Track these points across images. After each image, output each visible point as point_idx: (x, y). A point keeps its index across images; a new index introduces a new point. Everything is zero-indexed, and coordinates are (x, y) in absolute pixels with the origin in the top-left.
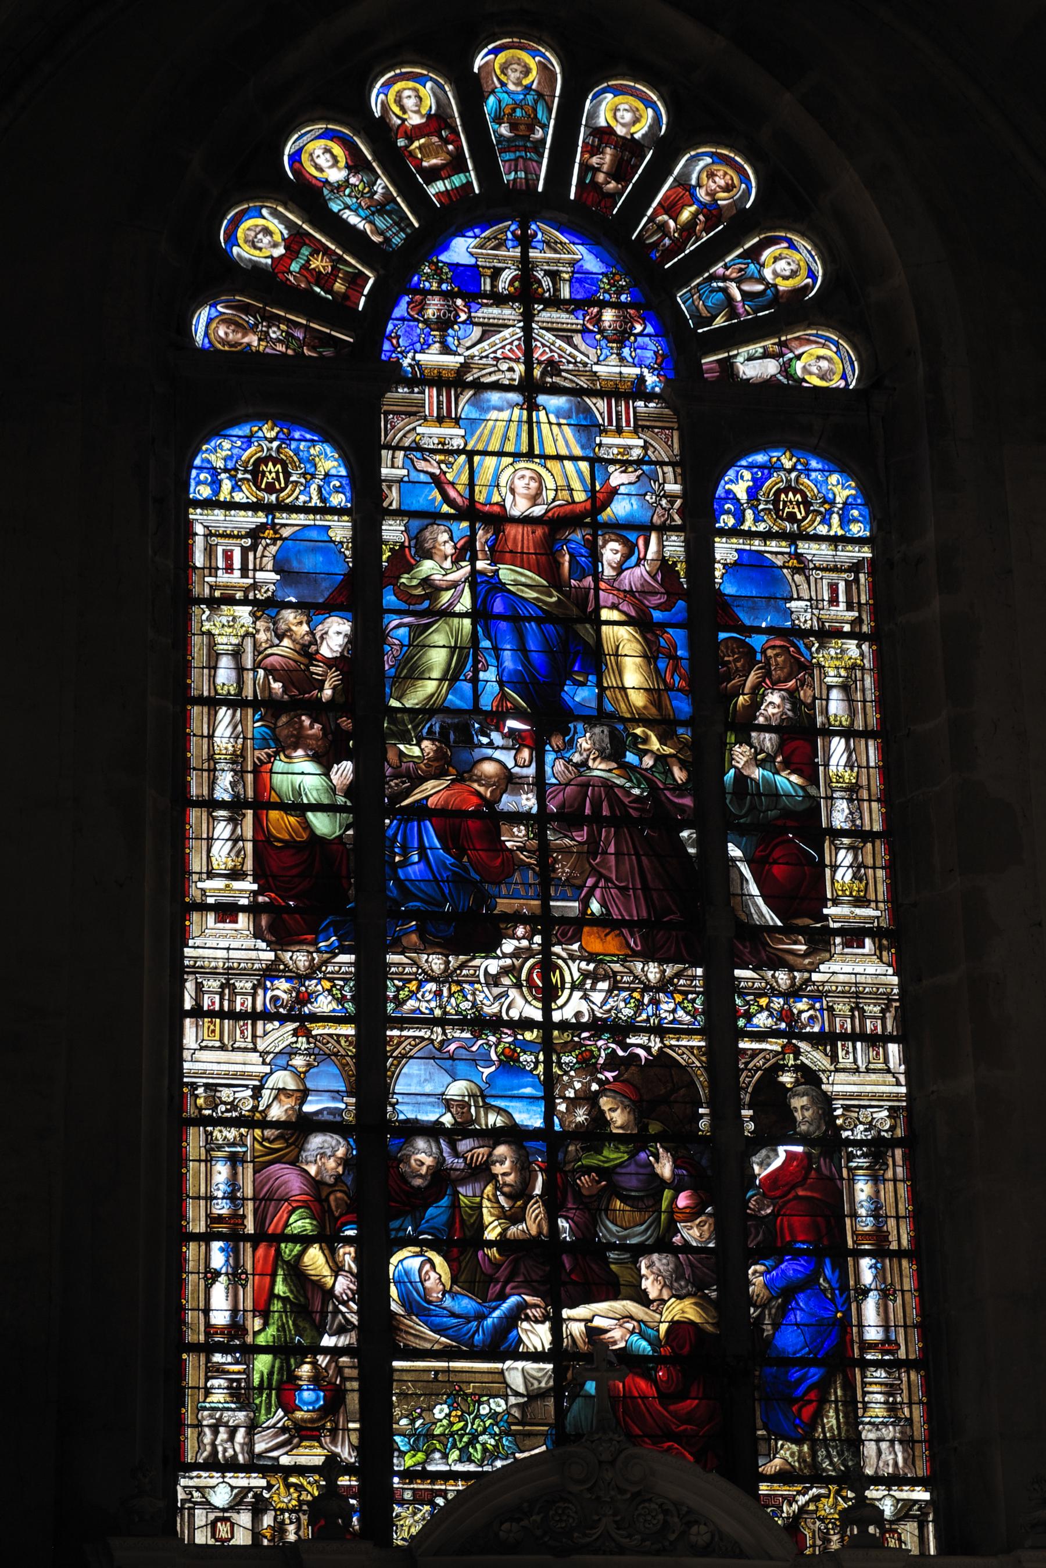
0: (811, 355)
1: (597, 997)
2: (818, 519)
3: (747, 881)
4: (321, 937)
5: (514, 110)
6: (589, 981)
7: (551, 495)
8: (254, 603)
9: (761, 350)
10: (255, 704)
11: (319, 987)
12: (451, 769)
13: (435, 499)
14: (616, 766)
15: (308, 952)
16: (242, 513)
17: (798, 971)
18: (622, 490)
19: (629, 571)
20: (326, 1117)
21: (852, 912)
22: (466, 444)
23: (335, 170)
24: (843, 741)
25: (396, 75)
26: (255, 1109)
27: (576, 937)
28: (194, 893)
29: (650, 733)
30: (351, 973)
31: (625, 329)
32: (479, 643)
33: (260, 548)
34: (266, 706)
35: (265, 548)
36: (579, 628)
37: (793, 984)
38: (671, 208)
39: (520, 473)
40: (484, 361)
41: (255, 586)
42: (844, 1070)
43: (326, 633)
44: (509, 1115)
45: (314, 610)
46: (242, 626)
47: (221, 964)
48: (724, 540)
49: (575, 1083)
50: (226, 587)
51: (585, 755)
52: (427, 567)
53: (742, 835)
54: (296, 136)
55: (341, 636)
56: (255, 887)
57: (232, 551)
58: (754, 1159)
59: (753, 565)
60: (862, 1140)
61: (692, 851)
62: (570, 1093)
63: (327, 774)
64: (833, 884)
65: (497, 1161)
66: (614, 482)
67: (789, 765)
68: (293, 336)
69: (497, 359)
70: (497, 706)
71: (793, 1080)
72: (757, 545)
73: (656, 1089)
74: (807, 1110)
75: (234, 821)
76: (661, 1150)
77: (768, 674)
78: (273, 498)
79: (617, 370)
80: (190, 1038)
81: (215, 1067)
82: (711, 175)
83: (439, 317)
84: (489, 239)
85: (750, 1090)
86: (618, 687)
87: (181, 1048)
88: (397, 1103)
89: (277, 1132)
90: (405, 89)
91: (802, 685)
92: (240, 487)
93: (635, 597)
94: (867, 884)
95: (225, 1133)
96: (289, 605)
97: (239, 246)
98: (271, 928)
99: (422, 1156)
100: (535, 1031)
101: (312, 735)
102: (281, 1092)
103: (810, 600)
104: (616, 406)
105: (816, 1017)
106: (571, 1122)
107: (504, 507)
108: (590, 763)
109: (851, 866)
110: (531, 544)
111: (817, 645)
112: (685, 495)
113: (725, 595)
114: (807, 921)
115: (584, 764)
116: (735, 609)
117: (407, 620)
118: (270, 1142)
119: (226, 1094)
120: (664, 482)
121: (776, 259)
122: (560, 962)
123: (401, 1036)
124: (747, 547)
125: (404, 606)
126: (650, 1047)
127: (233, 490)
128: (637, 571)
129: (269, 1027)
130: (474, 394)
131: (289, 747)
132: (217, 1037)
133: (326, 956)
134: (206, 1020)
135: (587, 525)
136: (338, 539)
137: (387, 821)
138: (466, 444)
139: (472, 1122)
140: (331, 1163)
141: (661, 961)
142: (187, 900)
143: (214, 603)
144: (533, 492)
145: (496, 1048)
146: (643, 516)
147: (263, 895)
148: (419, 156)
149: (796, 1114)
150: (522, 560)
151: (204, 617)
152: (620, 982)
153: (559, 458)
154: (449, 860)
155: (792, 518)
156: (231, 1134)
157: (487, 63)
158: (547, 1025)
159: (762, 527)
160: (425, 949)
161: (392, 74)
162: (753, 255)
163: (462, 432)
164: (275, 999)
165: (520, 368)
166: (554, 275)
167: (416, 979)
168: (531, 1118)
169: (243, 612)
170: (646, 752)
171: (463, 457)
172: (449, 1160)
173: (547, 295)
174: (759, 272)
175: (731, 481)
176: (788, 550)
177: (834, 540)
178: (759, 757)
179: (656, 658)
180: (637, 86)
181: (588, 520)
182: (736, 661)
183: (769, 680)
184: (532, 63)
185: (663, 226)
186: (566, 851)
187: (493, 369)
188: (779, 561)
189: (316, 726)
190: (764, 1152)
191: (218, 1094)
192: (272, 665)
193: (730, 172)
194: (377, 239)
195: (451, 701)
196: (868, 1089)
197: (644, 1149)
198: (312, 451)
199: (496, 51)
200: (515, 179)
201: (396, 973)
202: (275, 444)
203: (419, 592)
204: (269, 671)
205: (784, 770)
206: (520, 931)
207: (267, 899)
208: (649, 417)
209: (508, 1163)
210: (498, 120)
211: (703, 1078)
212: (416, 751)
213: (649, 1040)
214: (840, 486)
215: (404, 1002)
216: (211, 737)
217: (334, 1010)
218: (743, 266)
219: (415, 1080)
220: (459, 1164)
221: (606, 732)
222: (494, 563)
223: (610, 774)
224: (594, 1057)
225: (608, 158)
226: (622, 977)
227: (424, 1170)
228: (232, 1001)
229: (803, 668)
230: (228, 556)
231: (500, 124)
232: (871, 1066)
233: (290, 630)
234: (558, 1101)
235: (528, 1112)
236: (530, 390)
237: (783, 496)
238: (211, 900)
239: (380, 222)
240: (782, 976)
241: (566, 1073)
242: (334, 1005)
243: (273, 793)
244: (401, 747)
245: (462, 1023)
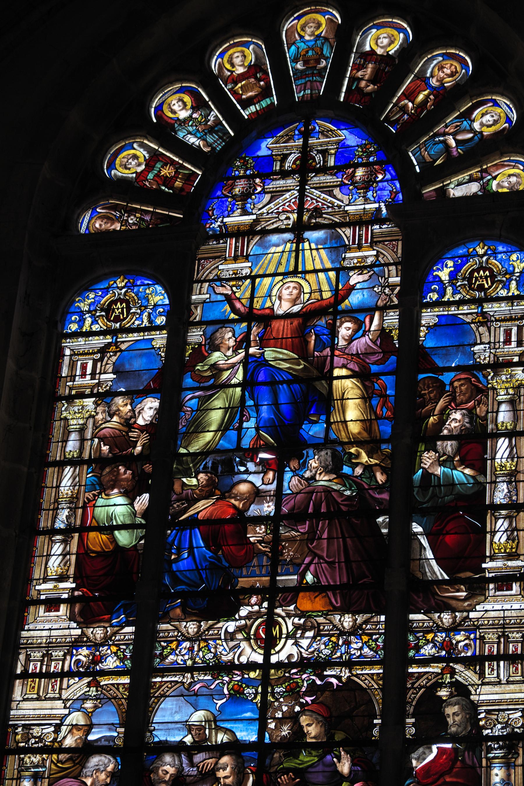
0: (504, 174)
1: (305, 643)
2: (501, 286)
3: (425, 548)
4: (114, 616)
5: (307, 52)
6: (299, 632)
7: (307, 296)
8: (98, 395)
9: (467, 178)
10: (89, 462)
11: (109, 651)
12: (217, 491)
13: (226, 310)
14: (335, 476)
15: (104, 627)
16: (97, 338)
17: (458, 612)
18: (358, 286)
19: (357, 341)
20: (104, 743)
21: (505, 565)
23: (184, 111)
24: (507, 440)
25: (230, 45)
26: (55, 740)
27: (294, 601)
28: (33, 593)
29: (361, 450)
30: (131, 639)
31: (371, 179)
32: (245, 403)
33: (106, 359)
34: (98, 462)
35: (109, 359)
36: (317, 384)
37: (454, 621)
38: (410, 95)
40: (270, 216)
41: (99, 384)
42: (488, 684)
43: (143, 409)
44: (233, 733)
45: (135, 395)
46: (88, 411)
47: (44, 641)
48: (429, 310)
49: (283, 707)
50: (80, 387)
51: (314, 472)
52: (216, 356)
53: (423, 516)
54: (161, 95)
55: (152, 410)
56: (74, 585)
57: (87, 363)
58: (413, 755)
59: (450, 325)
60: (499, 736)
61: (385, 531)
62: (279, 715)
63: (132, 504)
64: (491, 544)
65: (221, 768)
66: (352, 282)
67: (465, 462)
68: (143, 220)
69: (278, 213)
70: (253, 445)
71: (448, 693)
72: (453, 310)
73: (343, 708)
74: (458, 715)
75: (65, 542)
76: (343, 753)
77: (453, 399)
78: (118, 325)
79: (362, 207)
80: (17, 695)
81: (31, 712)
82: (441, 68)
83: (243, 192)
84: (282, 136)
85: (414, 703)
87: (11, 700)
88: (154, 730)
89: (67, 756)
90: (235, 53)
91: (479, 404)
92: (97, 321)
94: (518, 543)
95: (33, 759)
96: (121, 394)
97: (116, 169)
98: (82, 613)
99: (167, 768)
100: (258, 671)
101: (125, 478)
102: (75, 727)
103: (489, 343)
104: (359, 231)
105: (470, 645)
106: (277, 736)
107: (273, 309)
108: (317, 477)
109: (506, 531)
110: (289, 332)
111: (492, 374)
112: (402, 284)
113: (426, 348)
114: (469, 574)
115: (313, 478)
116: (433, 357)
117: (197, 394)
118: (63, 763)
119: (36, 731)
120: (389, 277)
121: (483, 115)
122: (280, 619)
123: (162, 682)
124: (446, 313)
125: (196, 385)
126: (342, 676)
127: (92, 324)
128: (363, 340)
129: (72, 681)
130: (260, 238)
131: (108, 488)
132: (36, 692)
133: (116, 629)
134: (30, 680)
135: (330, 313)
136: (158, 346)
137: (169, 532)
138: (251, 272)
139: (206, 740)
140: (103, 776)
141: (354, 613)
142: (28, 598)
143: (70, 399)
144: (294, 297)
145: (228, 685)
147: (78, 590)
148: (241, 92)
149: (448, 719)
150: (282, 343)
151: (63, 409)
152: (323, 630)
153: (315, 271)
154: (209, 554)
155: (481, 288)
156: (36, 759)
157: (292, 26)
158: (266, 666)
159: (457, 297)
160: (185, 618)
161: (228, 44)
162: (467, 115)
163: (249, 264)
164: (78, 661)
165: (294, 217)
166: (324, 153)
167: (177, 640)
168: (248, 734)
169: (89, 402)
170: (357, 464)
171: (249, 280)
172: (187, 769)
173: (318, 166)
174: (470, 126)
175: (438, 269)
176: (476, 311)
177: (511, 299)
178: (441, 459)
179: (370, 398)
180: (394, 20)
181: (331, 310)
182: (429, 393)
183: (455, 403)
184: (323, 20)
185: (404, 109)
186: (291, 540)
188: (468, 319)
189: (129, 472)
190: (421, 750)
191: (31, 731)
192: (104, 434)
193: (455, 64)
194: (206, 150)
195: (222, 445)
196: (508, 696)
197: (330, 752)
198: (147, 291)
199: (299, 18)
200: (303, 95)
201: (163, 637)
202: (124, 290)
203: (208, 374)
204: (101, 439)
205: (460, 466)
206: (254, 600)
207: (80, 593)
208: (382, 235)
209: (228, 769)
210: (295, 60)
211: (378, 696)
212: (194, 481)
213: (341, 671)
214: (519, 261)
215: (167, 657)
216: (58, 487)
217: (117, 667)
218: (459, 124)
219: (168, 713)
220: (194, 771)
221: (329, 454)
222: (262, 347)
223: (330, 483)
224: (299, 687)
225: (369, 70)
226: (324, 627)
227: (167, 777)
228: (48, 666)
229: (480, 392)
230: (84, 367)
231: (297, 63)
232: (511, 679)
233: (119, 410)
234: (269, 721)
235: (247, 730)
237: (476, 274)
238: (43, 597)
239: (210, 139)
240: (446, 616)
241: (277, 700)
242: (118, 663)
243: (94, 520)
244: (184, 480)
245: (206, 669)
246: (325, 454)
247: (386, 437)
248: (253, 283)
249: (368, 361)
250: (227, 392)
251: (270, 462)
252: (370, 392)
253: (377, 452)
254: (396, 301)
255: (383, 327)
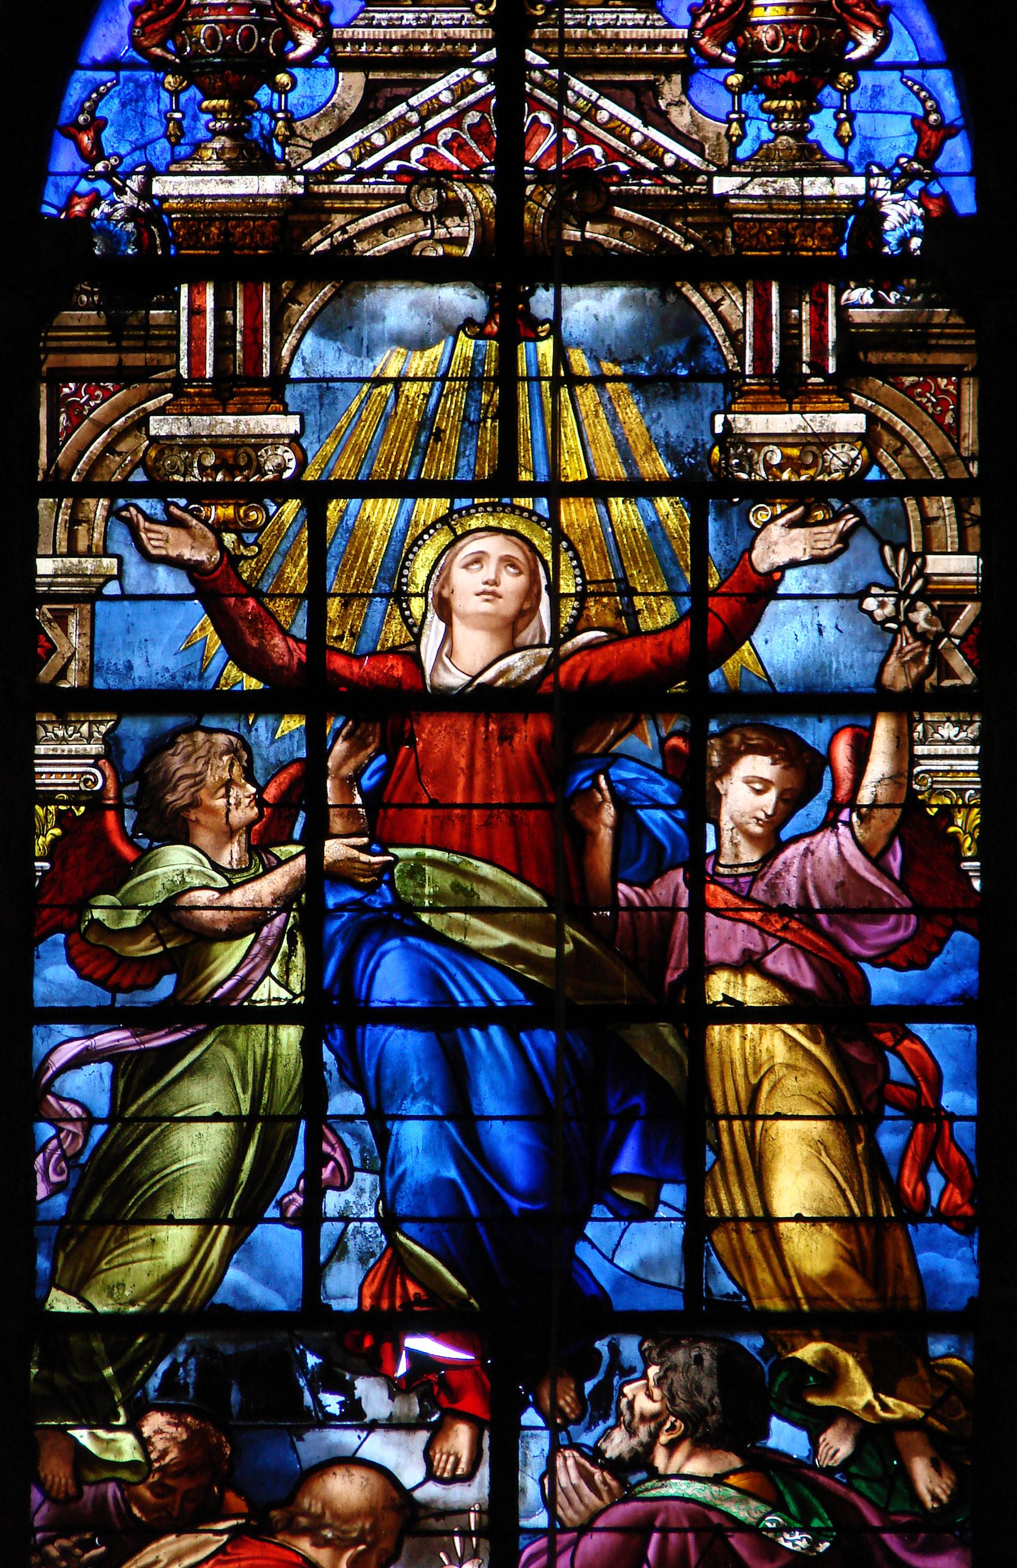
18: (792, 582)
22: (302, 464)
32: (324, 1100)
36: (638, 1035)
39: (471, 547)
51: (643, 1432)
66: (763, 559)
70: (377, 1297)
86: (751, 1218)
93: (816, 927)
107: (416, 659)
108: (660, 1459)
110: (499, 782)
112: (990, 588)
115: (641, 1460)
117: (106, 1040)
120: (927, 549)
125: (96, 996)
128: (826, 844)
130: (337, 295)
138: (302, 464)
144: (508, 606)
146: (852, 665)
163: (290, 424)
171: (292, 506)
179: (873, 1120)
187: (393, 211)
195: (237, 1291)
203: (145, 947)
208: (887, 336)
212: (126, 1447)
221: (707, 1360)
222: (380, 839)
236: (511, 268)
244: (82, 1436)
246: (694, 1359)
247: (954, 1301)
248: (315, 519)
249: (854, 946)
250: (240, 1041)
251: (455, 1379)
252: (869, 1090)
253: (914, 1370)
254: (963, 672)
255: (912, 794)
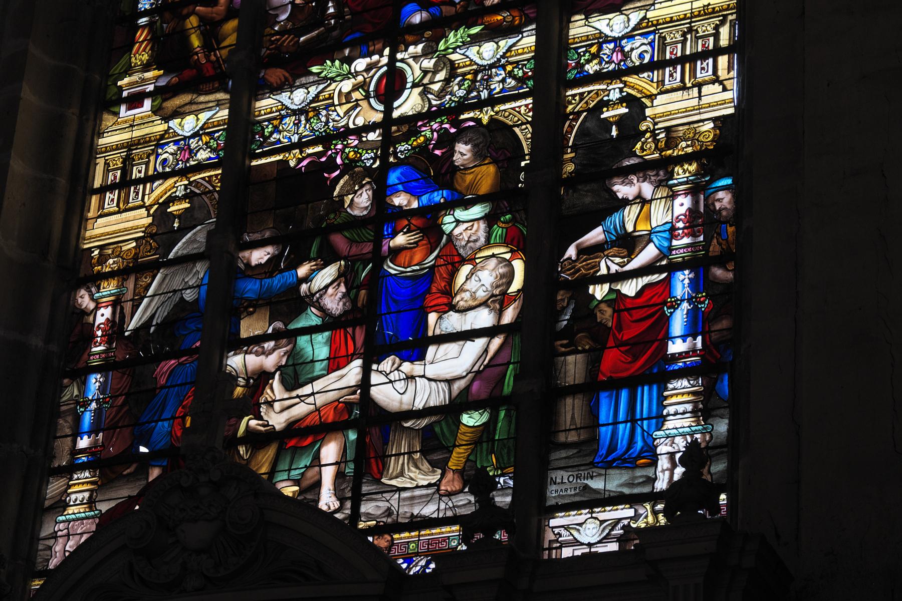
100: (378, 132)
